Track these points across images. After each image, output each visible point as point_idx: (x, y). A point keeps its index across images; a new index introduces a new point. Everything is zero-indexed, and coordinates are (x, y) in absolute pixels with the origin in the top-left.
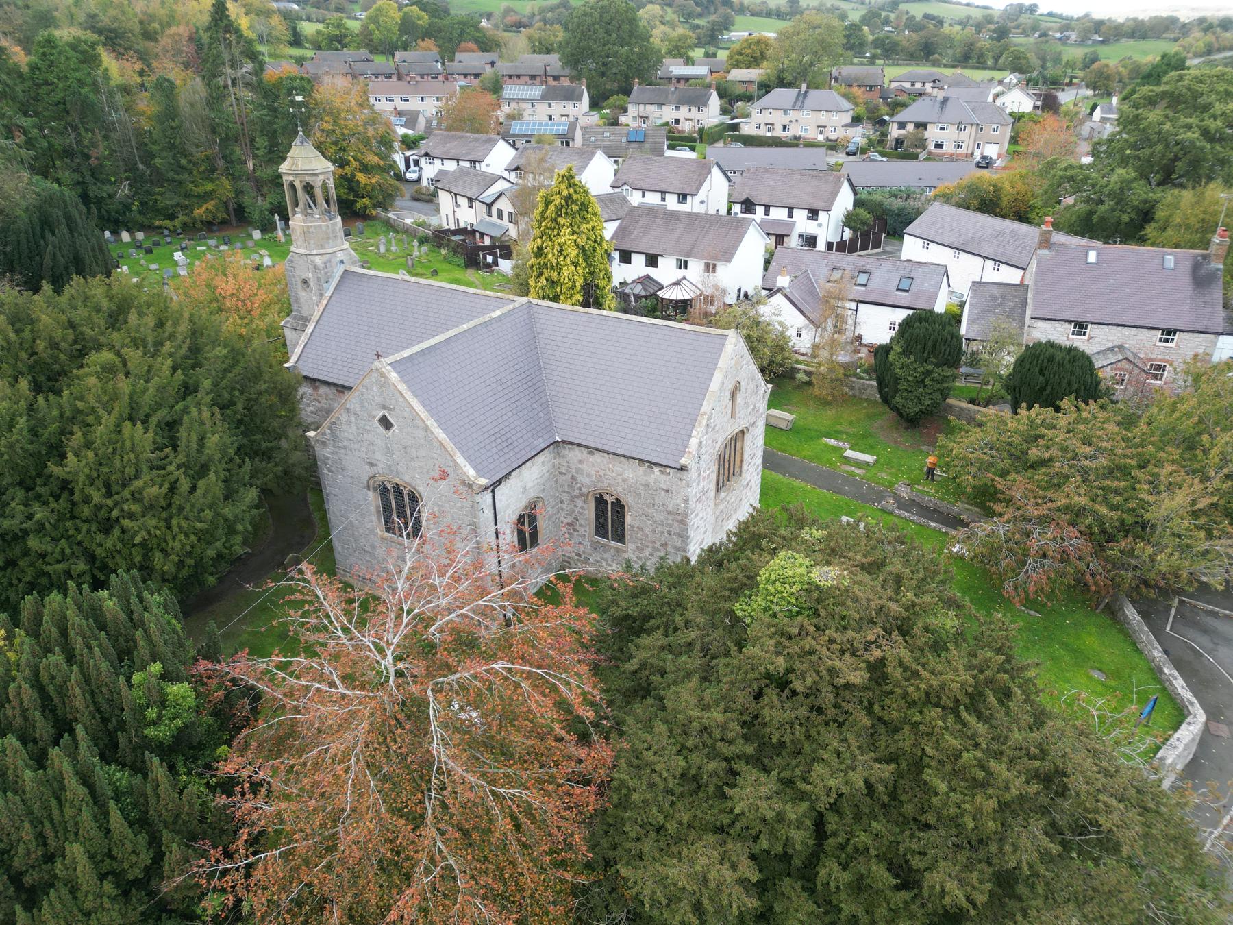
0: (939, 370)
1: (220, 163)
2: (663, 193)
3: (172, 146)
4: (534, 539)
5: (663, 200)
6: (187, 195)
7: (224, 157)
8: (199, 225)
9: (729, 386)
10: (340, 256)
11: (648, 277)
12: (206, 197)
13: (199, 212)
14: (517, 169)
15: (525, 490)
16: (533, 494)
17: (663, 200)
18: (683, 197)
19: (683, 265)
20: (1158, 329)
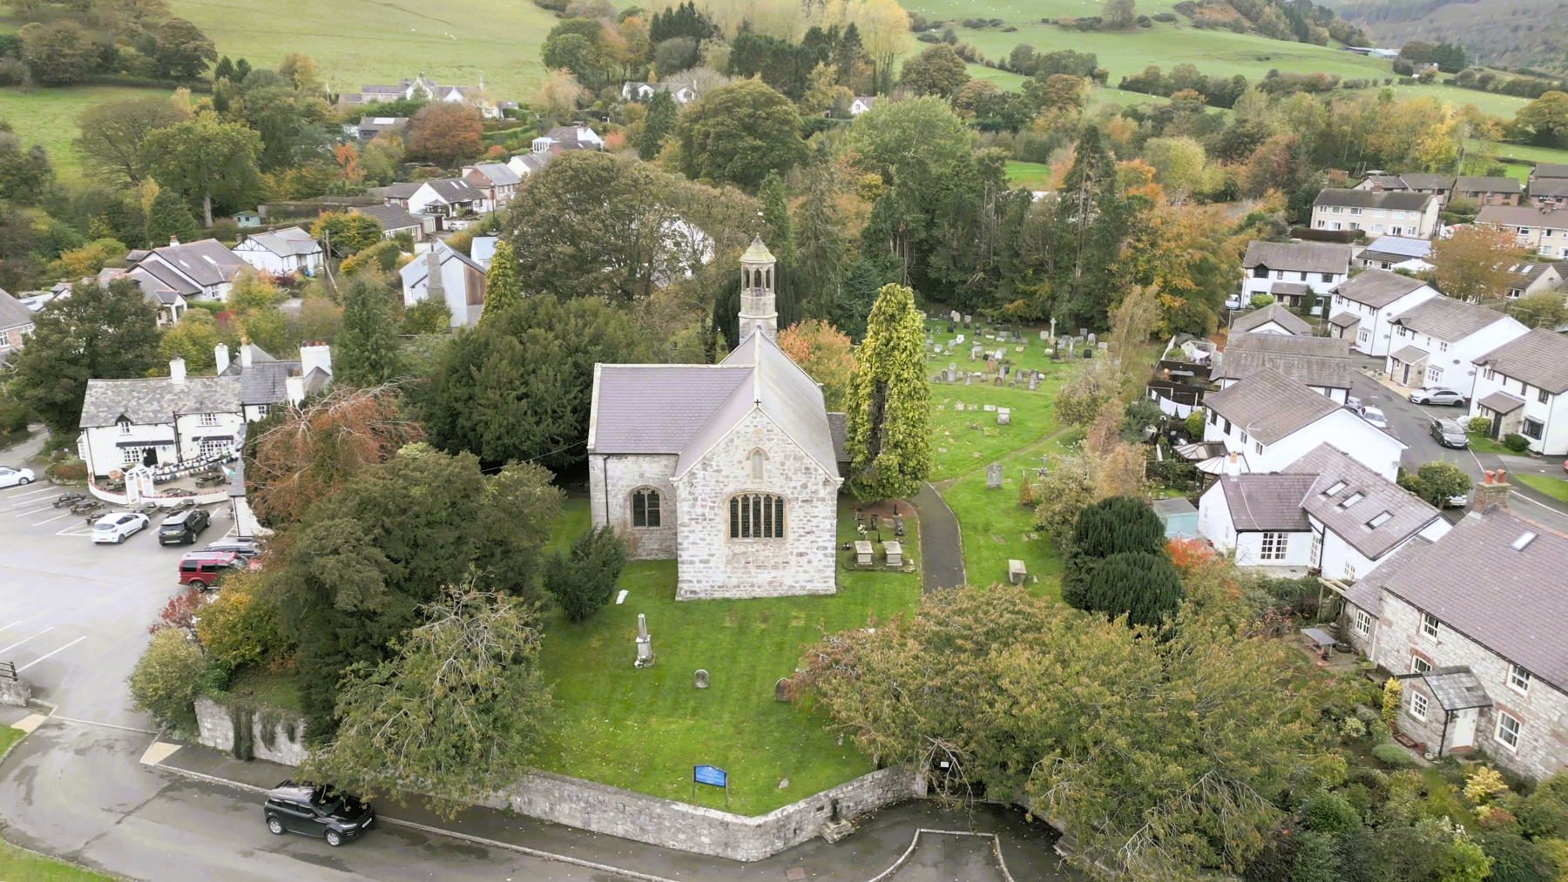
0: (1088, 558)
1: (1050, 266)
2: (1525, 384)
3: (1010, 247)
4: (655, 520)
5: (1523, 393)
6: (1015, 292)
7: (1056, 263)
8: (1015, 319)
9: (742, 448)
10: (759, 322)
11: (1222, 444)
12: (1025, 294)
13: (1009, 307)
14: (1398, 322)
15: (642, 476)
16: (652, 484)
17: (1523, 393)
18: (1544, 396)
19: (1244, 439)
20: (1510, 662)
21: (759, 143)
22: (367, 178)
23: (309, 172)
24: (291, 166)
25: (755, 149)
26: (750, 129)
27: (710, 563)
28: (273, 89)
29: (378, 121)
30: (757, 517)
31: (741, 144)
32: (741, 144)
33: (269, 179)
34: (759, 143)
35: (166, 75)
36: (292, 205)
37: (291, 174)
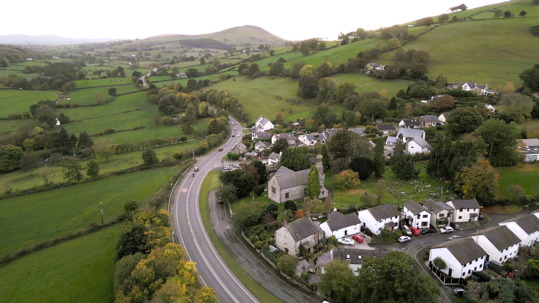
21: (457, 125)
22: (413, 114)
23: (398, 111)
24: (395, 109)
25: (455, 127)
26: (458, 121)
27: (270, 195)
28: (420, 86)
29: (440, 96)
30: (274, 190)
31: (453, 125)
32: (453, 125)
33: (388, 112)
34: (457, 125)
35: (415, 77)
36: (390, 118)
37: (394, 111)
